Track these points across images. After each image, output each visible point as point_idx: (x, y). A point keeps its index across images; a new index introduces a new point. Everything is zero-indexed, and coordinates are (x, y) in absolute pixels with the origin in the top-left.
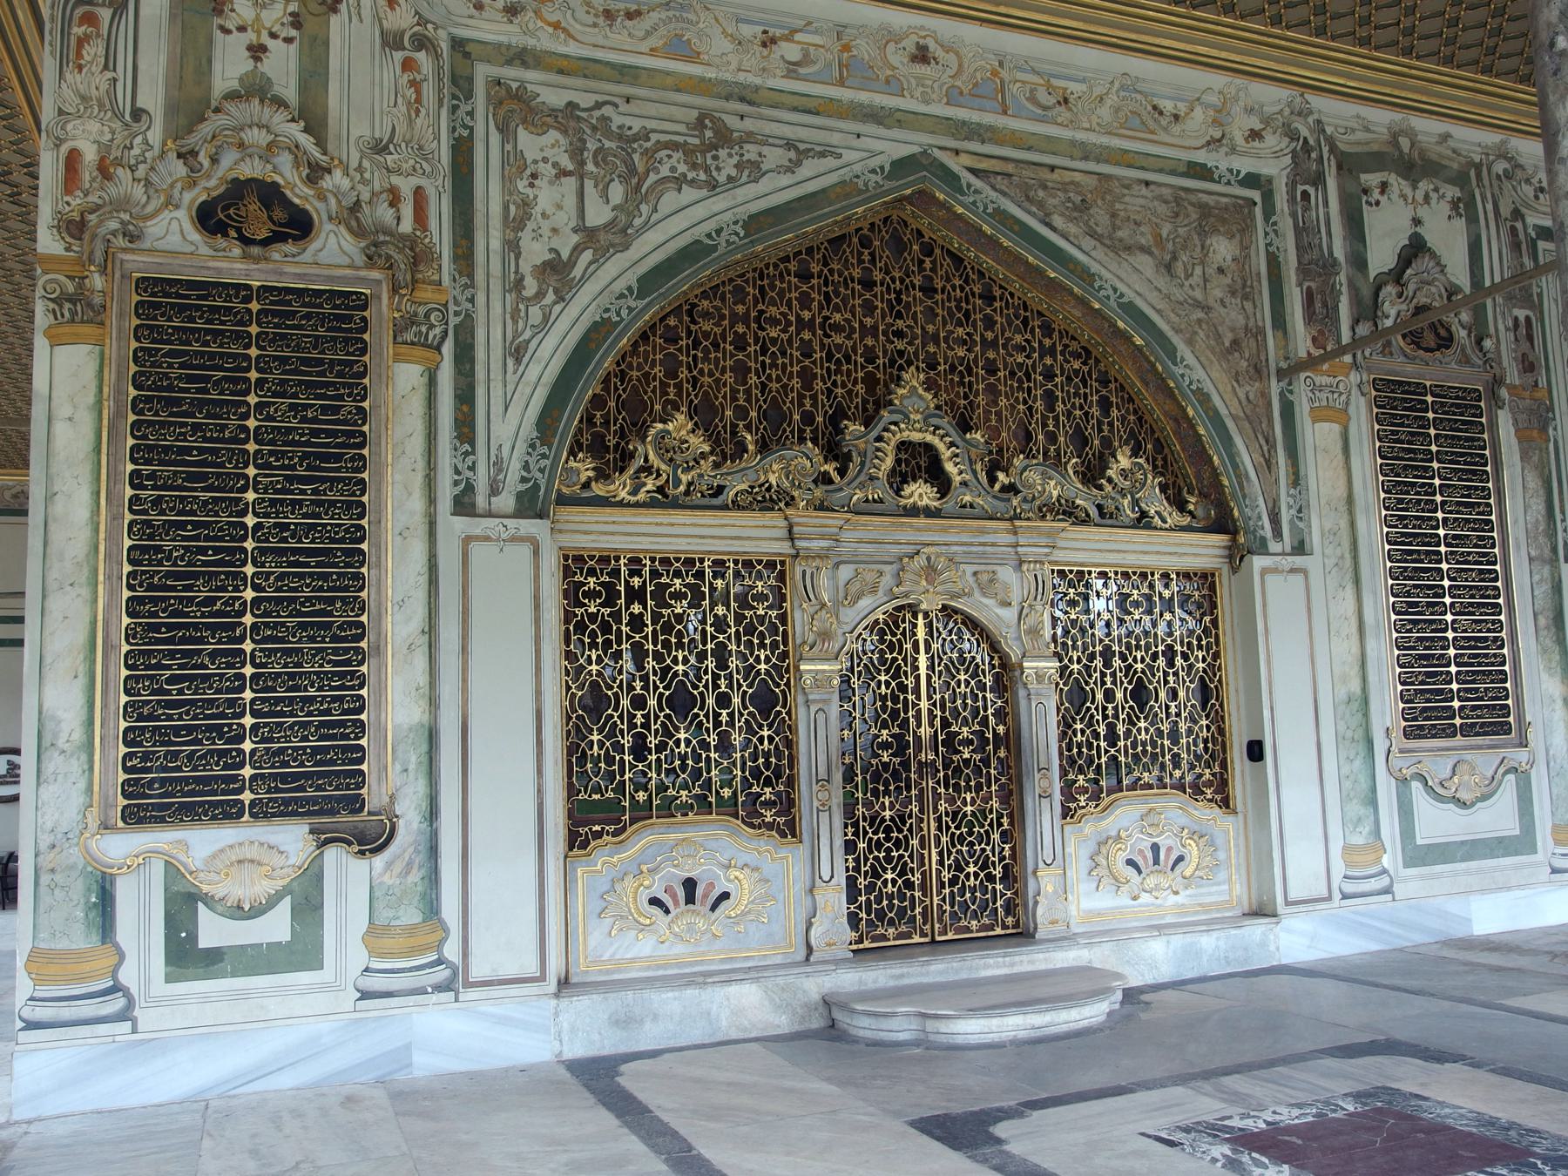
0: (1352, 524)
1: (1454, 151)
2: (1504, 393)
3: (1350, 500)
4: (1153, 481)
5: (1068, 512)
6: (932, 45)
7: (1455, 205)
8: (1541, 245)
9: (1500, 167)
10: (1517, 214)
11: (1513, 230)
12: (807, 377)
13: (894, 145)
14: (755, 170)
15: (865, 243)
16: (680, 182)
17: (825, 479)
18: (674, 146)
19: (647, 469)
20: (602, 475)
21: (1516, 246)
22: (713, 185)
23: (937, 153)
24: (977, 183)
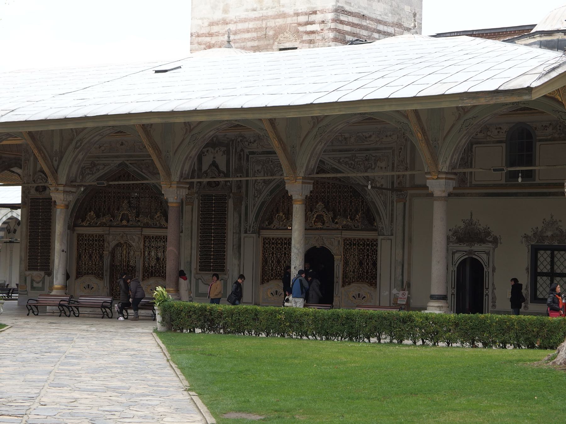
0: (192, 227)
1: (227, 138)
2: (231, 195)
3: (192, 221)
4: (163, 218)
5: (147, 226)
6: (124, 142)
7: (224, 152)
8: (250, 156)
9: (239, 140)
10: (242, 150)
11: (240, 155)
12: (114, 202)
13: (118, 161)
14: (98, 170)
15: (124, 176)
16: (89, 174)
17: (111, 220)
18: (87, 168)
19: (88, 220)
20: (83, 221)
21: (240, 159)
22: (93, 174)
23: (125, 162)
24: (131, 166)
